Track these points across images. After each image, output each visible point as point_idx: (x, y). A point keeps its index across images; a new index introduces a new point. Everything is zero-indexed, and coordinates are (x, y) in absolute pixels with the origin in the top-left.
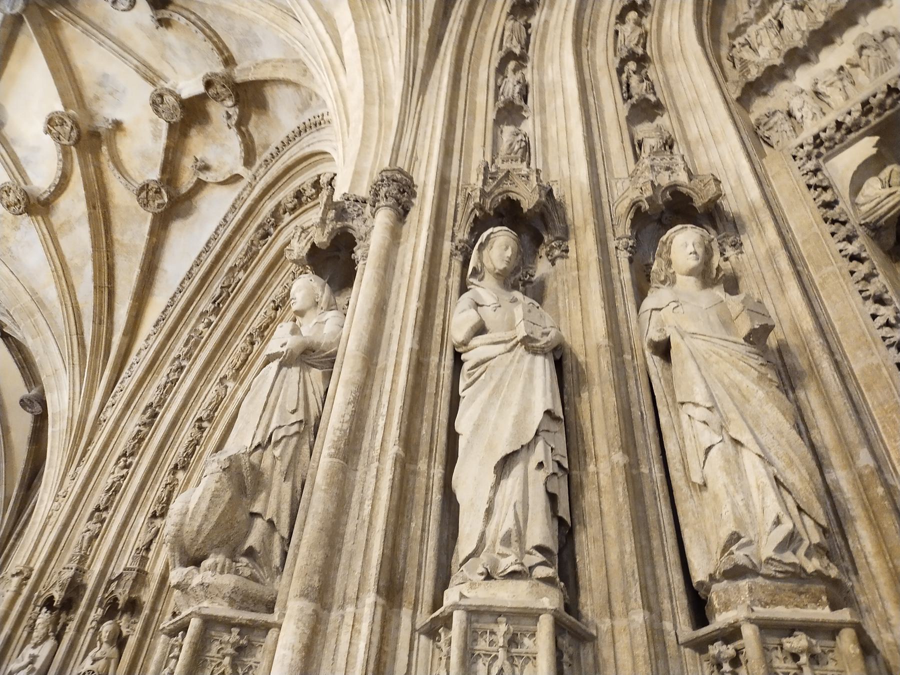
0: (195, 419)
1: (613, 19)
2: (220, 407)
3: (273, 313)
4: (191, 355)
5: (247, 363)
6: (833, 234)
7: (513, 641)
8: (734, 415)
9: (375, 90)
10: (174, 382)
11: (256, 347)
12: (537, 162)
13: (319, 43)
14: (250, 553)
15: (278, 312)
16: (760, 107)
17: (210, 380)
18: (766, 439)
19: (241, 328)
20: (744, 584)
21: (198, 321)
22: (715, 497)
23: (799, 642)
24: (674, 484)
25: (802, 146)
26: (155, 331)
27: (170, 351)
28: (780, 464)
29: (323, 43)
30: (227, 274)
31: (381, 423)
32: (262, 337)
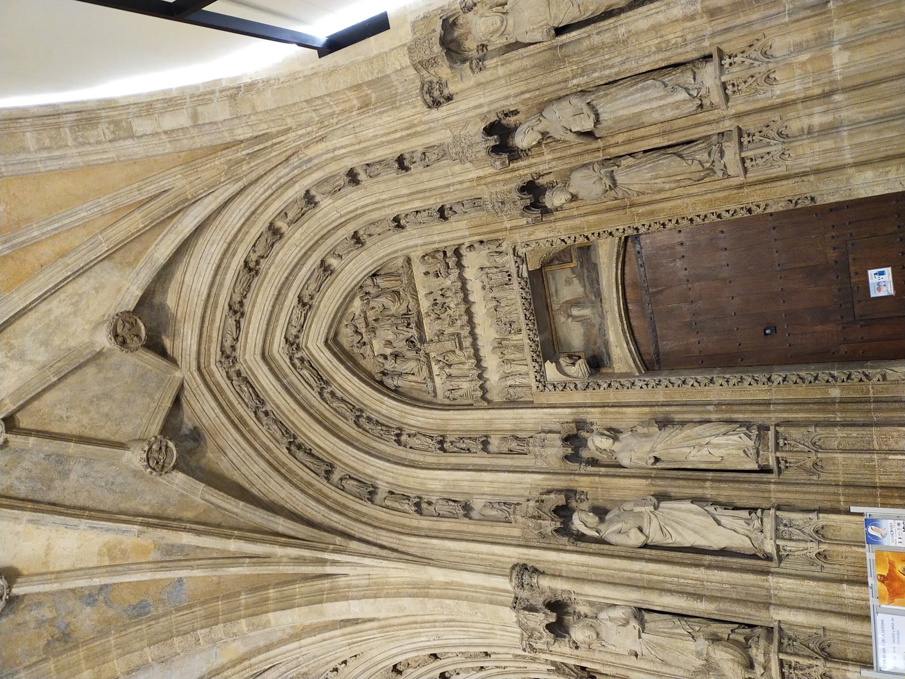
1: (400, 447)
6: (594, 389)
7: (785, 525)
8: (698, 441)
9: (415, 591)
12: (515, 500)
13: (322, 643)
14: (747, 639)
16: (495, 396)
18: (708, 434)
20: (761, 453)
22: (729, 455)
23: (781, 442)
24: (719, 468)
25: (538, 387)
28: (718, 432)
29: (324, 640)
31: (682, 581)
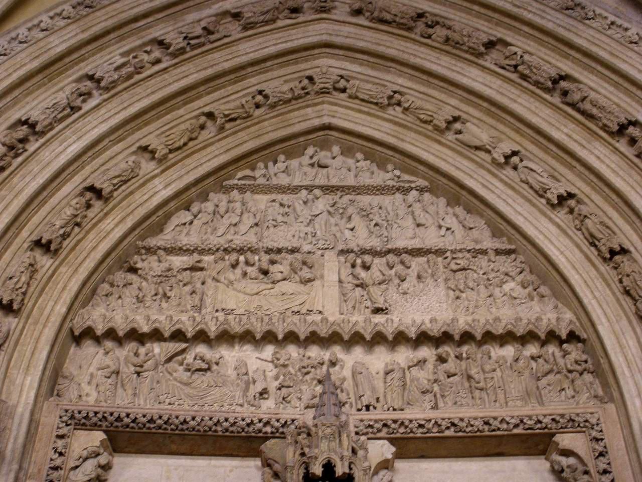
0: (86, 184)
2: (123, 187)
3: (250, 107)
4: (113, 87)
5: (186, 148)
10: (74, 109)
11: (205, 135)
15: (258, 112)
17: (124, 139)
19: (199, 97)
21: (145, 44)
26: (72, 15)
27: (82, 59)
30: (216, 15)
32: (222, 129)
